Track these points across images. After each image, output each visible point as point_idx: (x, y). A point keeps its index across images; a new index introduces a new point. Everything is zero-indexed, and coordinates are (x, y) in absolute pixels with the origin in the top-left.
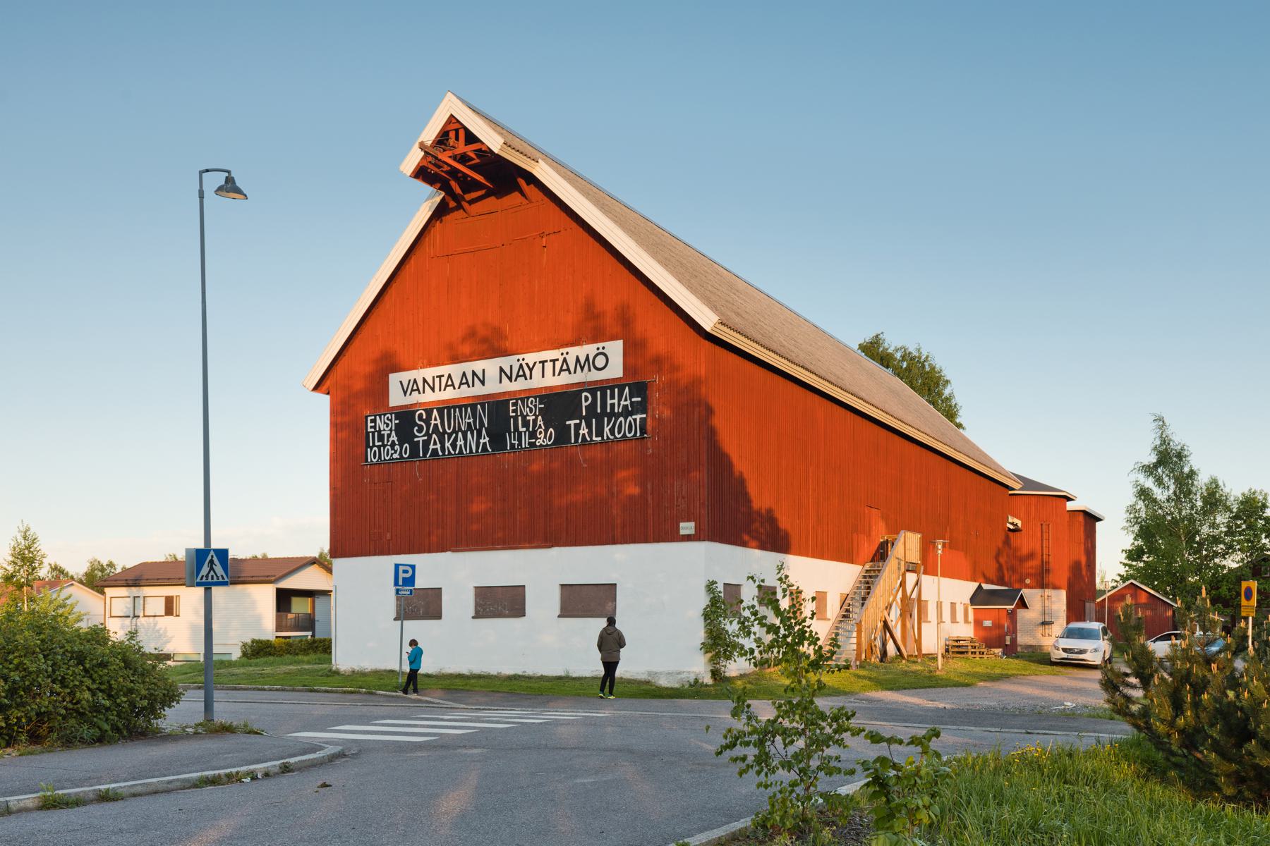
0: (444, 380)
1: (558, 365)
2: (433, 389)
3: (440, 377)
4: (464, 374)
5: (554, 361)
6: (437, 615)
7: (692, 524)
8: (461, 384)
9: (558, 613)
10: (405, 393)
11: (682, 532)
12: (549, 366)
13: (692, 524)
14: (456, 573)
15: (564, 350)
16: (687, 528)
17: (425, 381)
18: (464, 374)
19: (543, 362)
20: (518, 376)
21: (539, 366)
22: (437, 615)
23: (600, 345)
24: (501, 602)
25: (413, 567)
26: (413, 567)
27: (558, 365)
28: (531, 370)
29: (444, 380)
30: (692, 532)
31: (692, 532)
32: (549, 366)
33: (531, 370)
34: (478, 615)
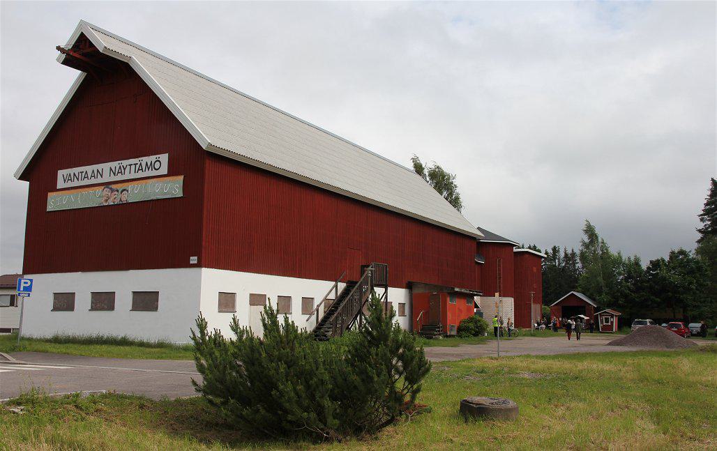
0: (83, 174)
1: (137, 166)
2: (78, 179)
3: (82, 172)
4: (93, 171)
5: (136, 164)
6: (252, 295)
7: (196, 258)
8: (91, 176)
9: (131, 308)
10: (65, 181)
11: (191, 262)
12: (133, 167)
13: (196, 258)
14: (82, 284)
15: (140, 159)
16: (194, 260)
17: (74, 175)
18: (93, 171)
19: (130, 165)
20: (118, 173)
21: (128, 167)
22: (252, 295)
23: (158, 156)
24: (103, 301)
25: (31, 281)
26: (31, 281)
27: (137, 166)
28: (125, 169)
29: (83, 174)
30: (196, 262)
31: (196, 262)
32: (133, 167)
33: (125, 169)
34: (93, 309)
